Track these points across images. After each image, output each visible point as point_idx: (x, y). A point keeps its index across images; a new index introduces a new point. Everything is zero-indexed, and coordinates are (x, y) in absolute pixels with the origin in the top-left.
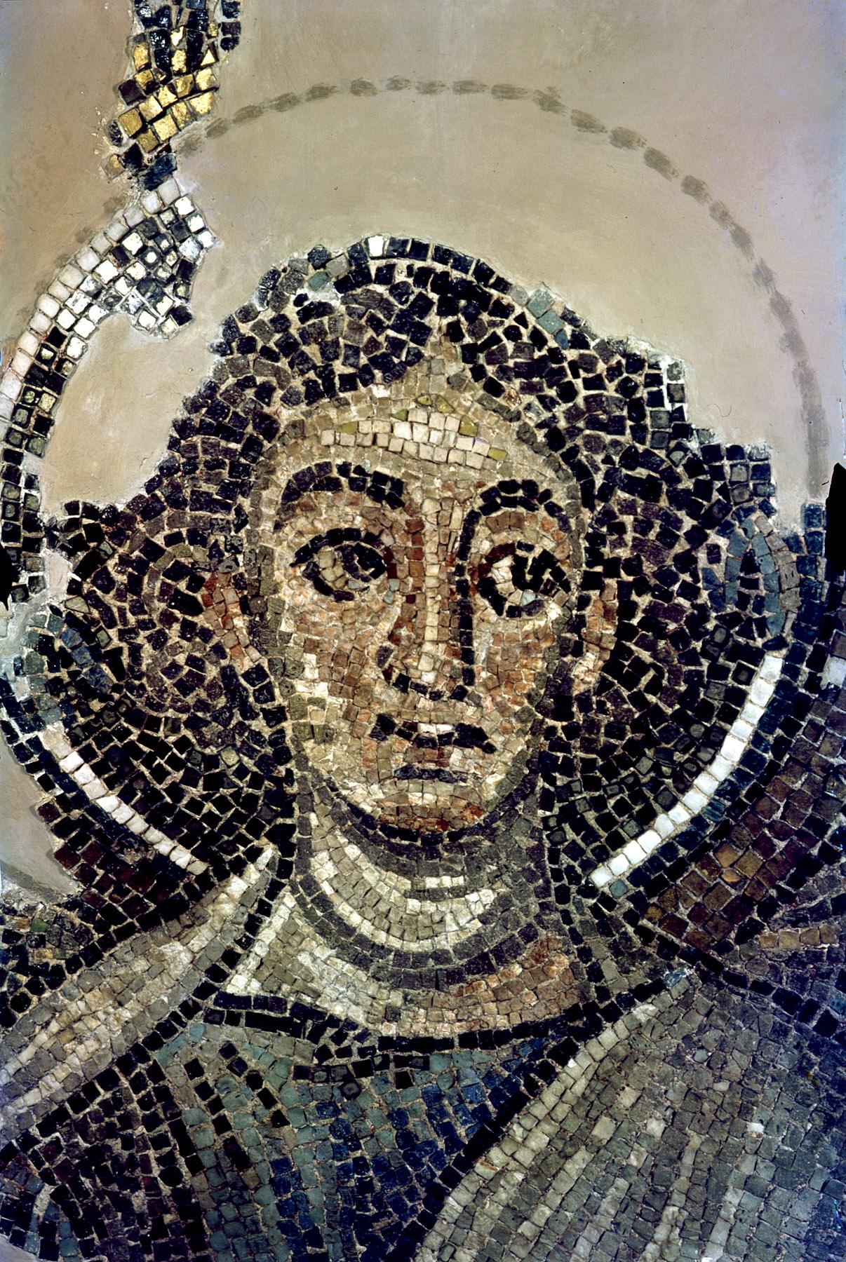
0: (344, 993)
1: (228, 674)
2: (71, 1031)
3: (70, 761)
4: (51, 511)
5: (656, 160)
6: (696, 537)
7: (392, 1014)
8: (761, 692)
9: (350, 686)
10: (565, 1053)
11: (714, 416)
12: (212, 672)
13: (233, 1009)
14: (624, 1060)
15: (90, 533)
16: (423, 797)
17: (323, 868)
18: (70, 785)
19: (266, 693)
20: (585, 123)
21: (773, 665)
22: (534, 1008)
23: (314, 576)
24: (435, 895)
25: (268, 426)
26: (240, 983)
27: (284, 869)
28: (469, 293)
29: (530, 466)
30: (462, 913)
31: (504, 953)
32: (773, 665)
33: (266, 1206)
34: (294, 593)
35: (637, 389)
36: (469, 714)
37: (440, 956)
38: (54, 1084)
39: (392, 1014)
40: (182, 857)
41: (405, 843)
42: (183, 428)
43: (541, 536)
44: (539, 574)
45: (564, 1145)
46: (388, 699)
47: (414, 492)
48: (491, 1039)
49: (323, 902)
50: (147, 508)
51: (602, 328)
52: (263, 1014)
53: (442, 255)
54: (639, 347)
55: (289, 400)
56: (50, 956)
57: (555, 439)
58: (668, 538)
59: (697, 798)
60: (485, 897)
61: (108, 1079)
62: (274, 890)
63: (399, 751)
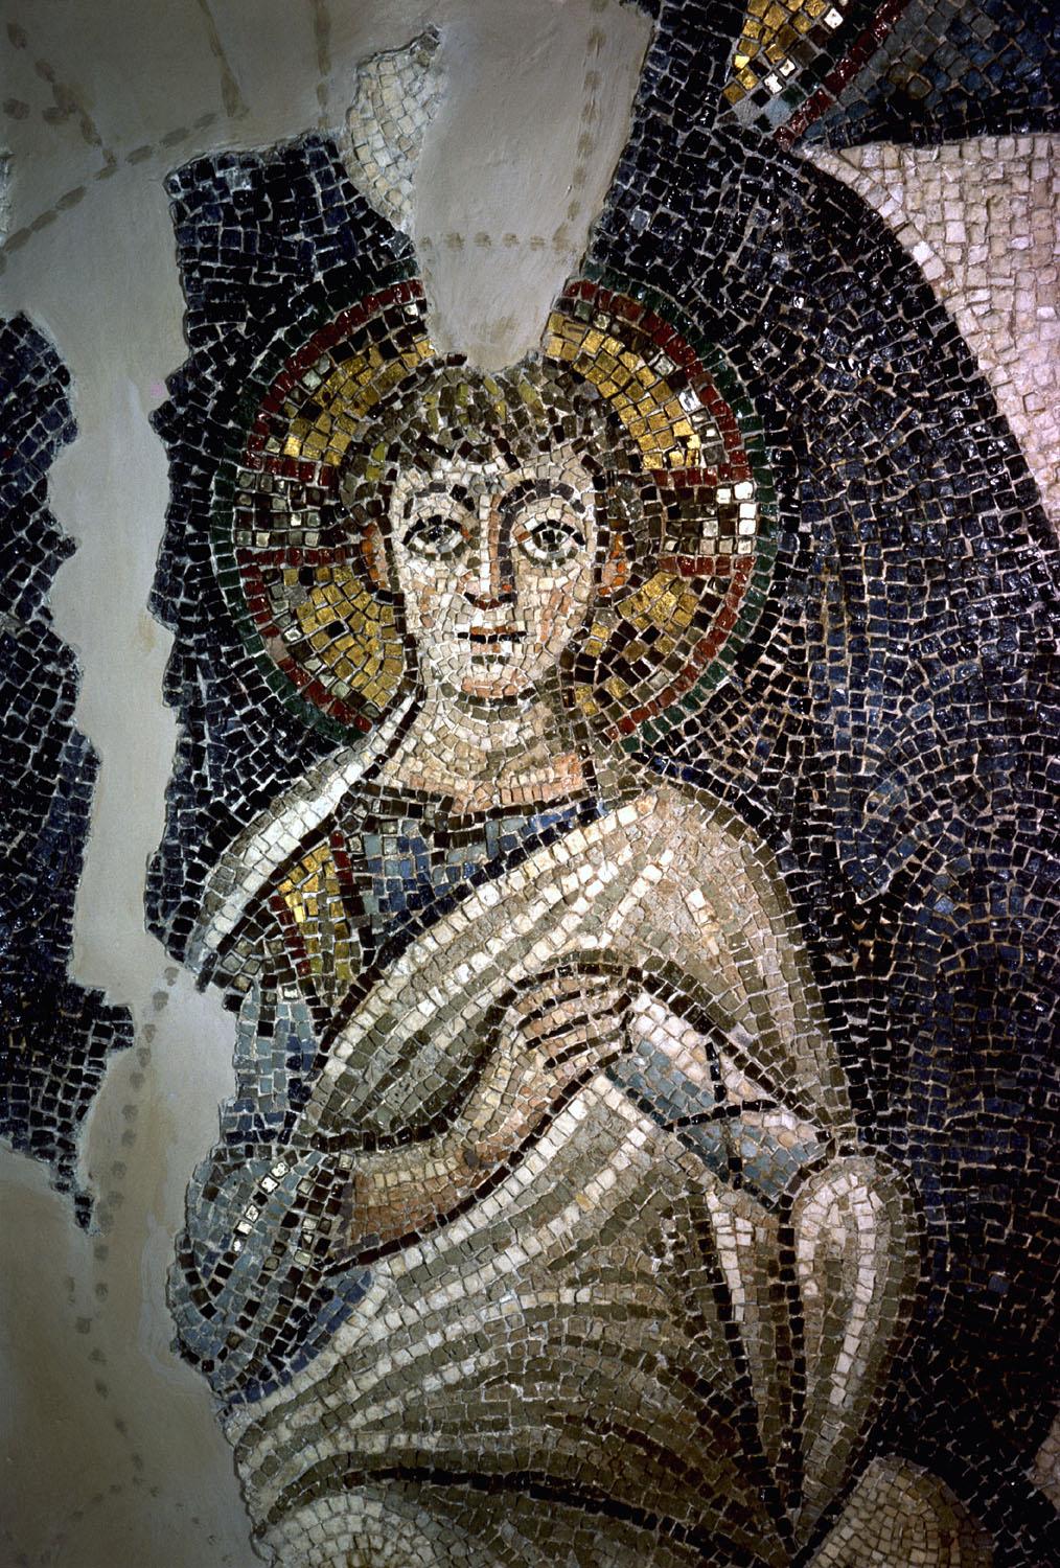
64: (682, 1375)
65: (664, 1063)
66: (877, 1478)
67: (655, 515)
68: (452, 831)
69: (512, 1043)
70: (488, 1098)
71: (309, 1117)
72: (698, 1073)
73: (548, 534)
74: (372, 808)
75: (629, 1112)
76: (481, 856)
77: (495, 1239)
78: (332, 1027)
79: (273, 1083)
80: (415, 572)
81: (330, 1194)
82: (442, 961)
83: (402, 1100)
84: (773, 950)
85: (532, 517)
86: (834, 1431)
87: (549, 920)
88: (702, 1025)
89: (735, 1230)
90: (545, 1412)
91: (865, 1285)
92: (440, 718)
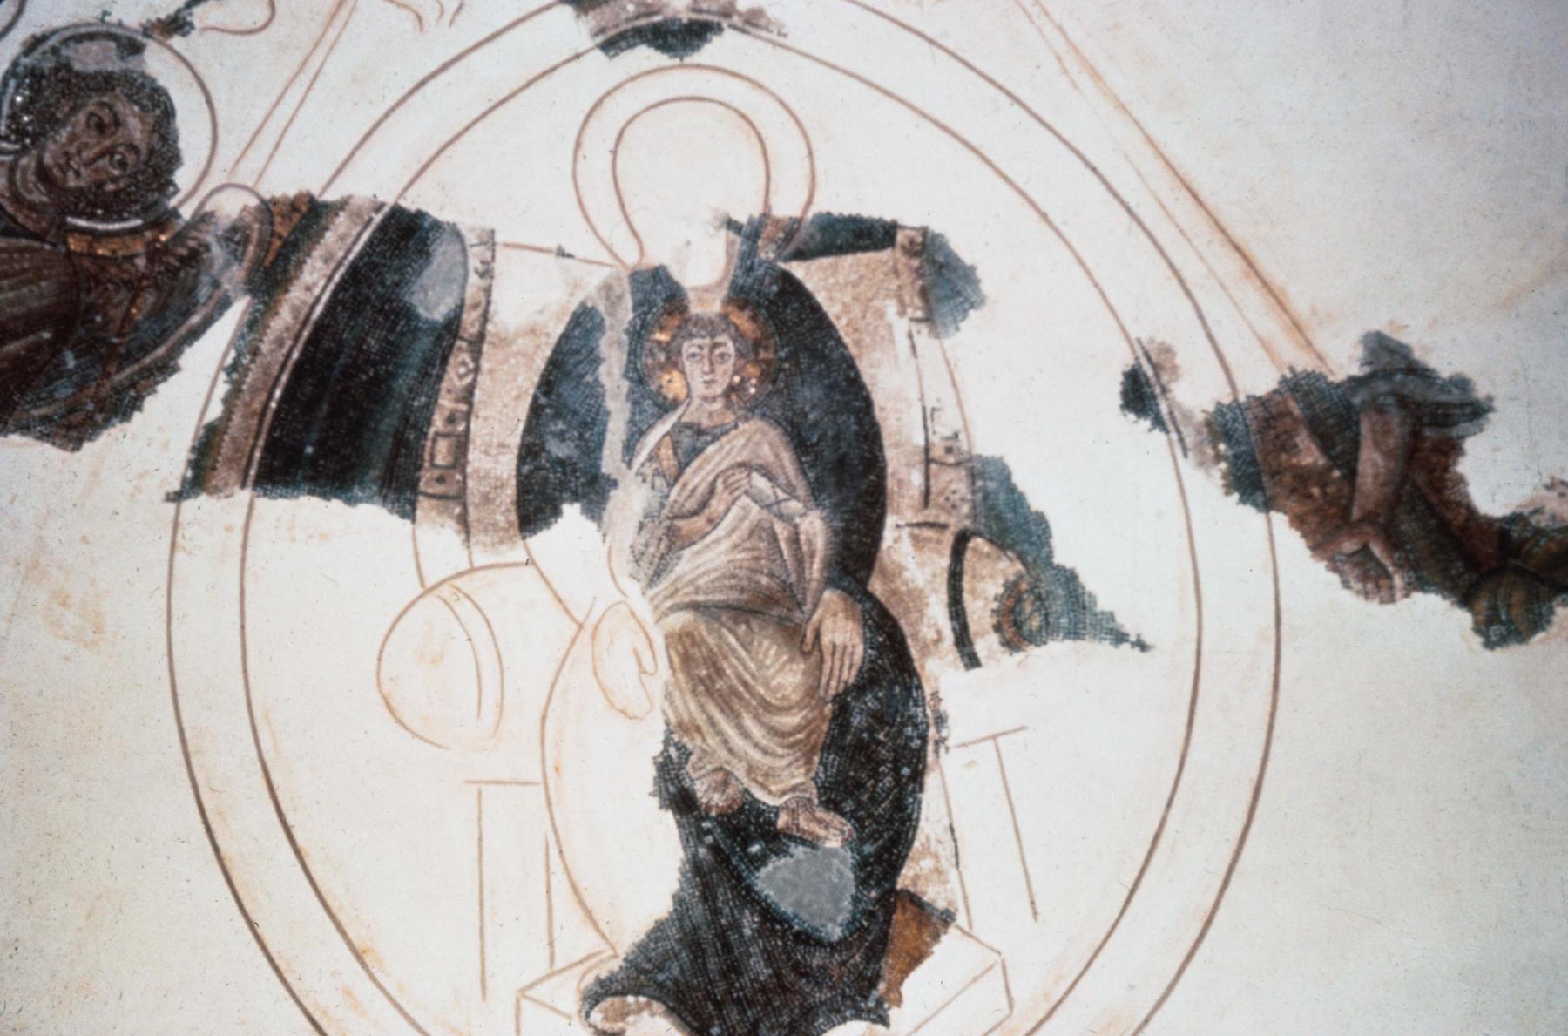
16: (56, 172)
17: (24, 161)
21: (139, 222)
22: (30, 225)
23: (88, 119)
25: (113, 89)
29: (144, 149)
30: (39, 196)
31: (37, 211)
32: (139, 222)
34: (81, 117)
35: (174, 159)
36: (83, 170)
41: (43, 174)
43: (131, 159)
44: (122, 164)
46: (73, 150)
59: (101, 227)
60: (45, 199)
63: (62, 161)
64: (771, 575)
65: (761, 491)
66: (828, 594)
67: (750, 350)
68: (699, 431)
69: (719, 485)
70: (714, 502)
71: (665, 512)
72: (770, 492)
73: (722, 356)
74: (680, 427)
75: (752, 504)
76: (709, 438)
77: (717, 541)
78: (671, 486)
79: (656, 505)
80: (688, 366)
81: (672, 532)
82: (700, 467)
83: (691, 505)
84: (787, 457)
85: (717, 351)
86: (814, 585)
87: (728, 454)
88: (770, 479)
89: (782, 531)
90: (731, 587)
91: (820, 543)
92: (696, 401)
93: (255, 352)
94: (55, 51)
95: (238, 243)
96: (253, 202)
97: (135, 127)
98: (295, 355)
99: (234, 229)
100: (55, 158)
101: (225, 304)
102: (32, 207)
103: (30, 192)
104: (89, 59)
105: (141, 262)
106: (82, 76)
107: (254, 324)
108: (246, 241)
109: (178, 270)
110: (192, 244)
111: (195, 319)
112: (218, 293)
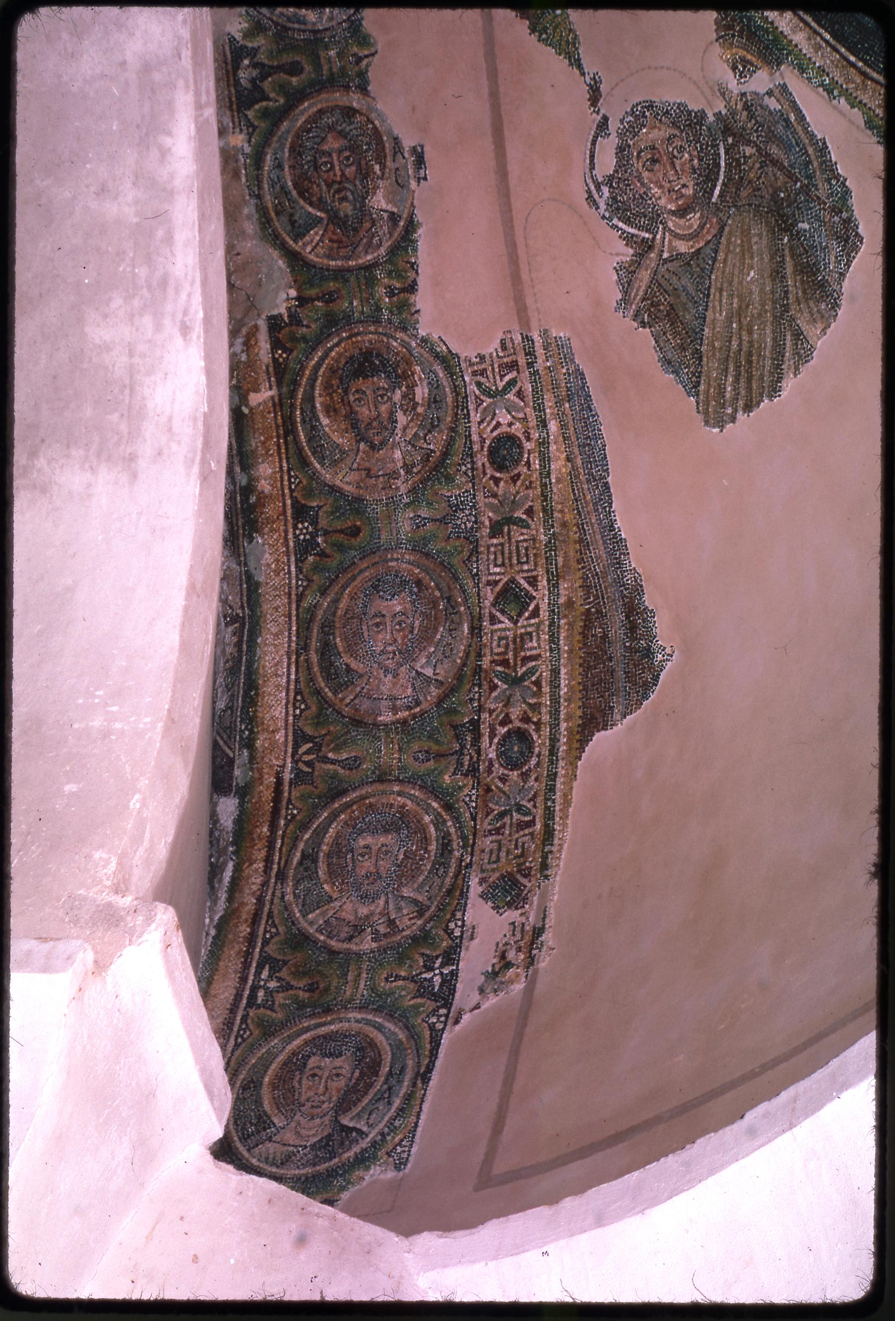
0: (683, 247)
1: (640, 195)
2: (641, 281)
3: (621, 224)
4: (600, 179)
5: (668, 69)
6: (700, 129)
7: (692, 247)
8: (722, 152)
9: (661, 187)
10: (721, 236)
11: (694, 107)
12: (637, 196)
13: (666, 261)
14: (730, 233)
15: (609, 180)
17: (670, 224)
18: (621, 229)
19: (647, 196)
20: (656, 68)
22: (714, 231)
24: (690, 218)
25: (629, 146)
26: (666, 255)
27: (664, 229)
28: (651, 106)
31: (705, 224)
33: (684, 298)
36: (682, 182)
37: (695, 231)
38: (641, 293)
39: (692, 247)
40: (647, 235)
41: (682, 212)
42: (617, 154)
44: (681, 150)
45: (726, 255)
47: (657, 146)
48: (709, 242)
49: (673, 231)
50: (616, 171)
51: (672, 101)
52: (670, 260)
53: (644, 102)
54: (678, 101)
55: (631, 140)
56: (632, 268)
57: (673, 124)
58: (696, 131)
59: (722, 177)
60: (698, 215)
61: (650, 287)
62: (664, 234)
93: (822, 70)
94: (598, 187)
95: (744, 67)
96: (717, 49)
97: (653, 134)
98: (828, 37)
99: (734, 68)
100: (670, 200)
101: (784, 88)
102: (702, 226)
103: (691, 226)
104: (607, 163)
105: (749, 151)
106: (619, 166)
107: (802, 70)
108: (745, 62)
109: (756, 120)
110: (739, 107)
111: (792, 117)
112: (776, 92)
